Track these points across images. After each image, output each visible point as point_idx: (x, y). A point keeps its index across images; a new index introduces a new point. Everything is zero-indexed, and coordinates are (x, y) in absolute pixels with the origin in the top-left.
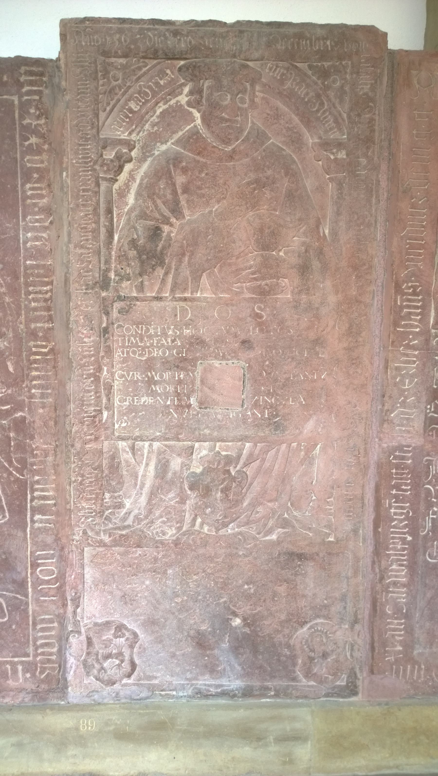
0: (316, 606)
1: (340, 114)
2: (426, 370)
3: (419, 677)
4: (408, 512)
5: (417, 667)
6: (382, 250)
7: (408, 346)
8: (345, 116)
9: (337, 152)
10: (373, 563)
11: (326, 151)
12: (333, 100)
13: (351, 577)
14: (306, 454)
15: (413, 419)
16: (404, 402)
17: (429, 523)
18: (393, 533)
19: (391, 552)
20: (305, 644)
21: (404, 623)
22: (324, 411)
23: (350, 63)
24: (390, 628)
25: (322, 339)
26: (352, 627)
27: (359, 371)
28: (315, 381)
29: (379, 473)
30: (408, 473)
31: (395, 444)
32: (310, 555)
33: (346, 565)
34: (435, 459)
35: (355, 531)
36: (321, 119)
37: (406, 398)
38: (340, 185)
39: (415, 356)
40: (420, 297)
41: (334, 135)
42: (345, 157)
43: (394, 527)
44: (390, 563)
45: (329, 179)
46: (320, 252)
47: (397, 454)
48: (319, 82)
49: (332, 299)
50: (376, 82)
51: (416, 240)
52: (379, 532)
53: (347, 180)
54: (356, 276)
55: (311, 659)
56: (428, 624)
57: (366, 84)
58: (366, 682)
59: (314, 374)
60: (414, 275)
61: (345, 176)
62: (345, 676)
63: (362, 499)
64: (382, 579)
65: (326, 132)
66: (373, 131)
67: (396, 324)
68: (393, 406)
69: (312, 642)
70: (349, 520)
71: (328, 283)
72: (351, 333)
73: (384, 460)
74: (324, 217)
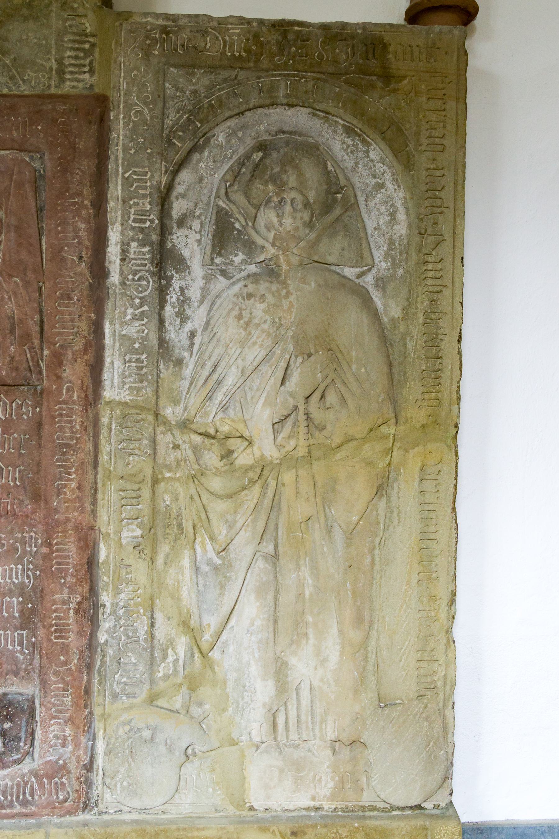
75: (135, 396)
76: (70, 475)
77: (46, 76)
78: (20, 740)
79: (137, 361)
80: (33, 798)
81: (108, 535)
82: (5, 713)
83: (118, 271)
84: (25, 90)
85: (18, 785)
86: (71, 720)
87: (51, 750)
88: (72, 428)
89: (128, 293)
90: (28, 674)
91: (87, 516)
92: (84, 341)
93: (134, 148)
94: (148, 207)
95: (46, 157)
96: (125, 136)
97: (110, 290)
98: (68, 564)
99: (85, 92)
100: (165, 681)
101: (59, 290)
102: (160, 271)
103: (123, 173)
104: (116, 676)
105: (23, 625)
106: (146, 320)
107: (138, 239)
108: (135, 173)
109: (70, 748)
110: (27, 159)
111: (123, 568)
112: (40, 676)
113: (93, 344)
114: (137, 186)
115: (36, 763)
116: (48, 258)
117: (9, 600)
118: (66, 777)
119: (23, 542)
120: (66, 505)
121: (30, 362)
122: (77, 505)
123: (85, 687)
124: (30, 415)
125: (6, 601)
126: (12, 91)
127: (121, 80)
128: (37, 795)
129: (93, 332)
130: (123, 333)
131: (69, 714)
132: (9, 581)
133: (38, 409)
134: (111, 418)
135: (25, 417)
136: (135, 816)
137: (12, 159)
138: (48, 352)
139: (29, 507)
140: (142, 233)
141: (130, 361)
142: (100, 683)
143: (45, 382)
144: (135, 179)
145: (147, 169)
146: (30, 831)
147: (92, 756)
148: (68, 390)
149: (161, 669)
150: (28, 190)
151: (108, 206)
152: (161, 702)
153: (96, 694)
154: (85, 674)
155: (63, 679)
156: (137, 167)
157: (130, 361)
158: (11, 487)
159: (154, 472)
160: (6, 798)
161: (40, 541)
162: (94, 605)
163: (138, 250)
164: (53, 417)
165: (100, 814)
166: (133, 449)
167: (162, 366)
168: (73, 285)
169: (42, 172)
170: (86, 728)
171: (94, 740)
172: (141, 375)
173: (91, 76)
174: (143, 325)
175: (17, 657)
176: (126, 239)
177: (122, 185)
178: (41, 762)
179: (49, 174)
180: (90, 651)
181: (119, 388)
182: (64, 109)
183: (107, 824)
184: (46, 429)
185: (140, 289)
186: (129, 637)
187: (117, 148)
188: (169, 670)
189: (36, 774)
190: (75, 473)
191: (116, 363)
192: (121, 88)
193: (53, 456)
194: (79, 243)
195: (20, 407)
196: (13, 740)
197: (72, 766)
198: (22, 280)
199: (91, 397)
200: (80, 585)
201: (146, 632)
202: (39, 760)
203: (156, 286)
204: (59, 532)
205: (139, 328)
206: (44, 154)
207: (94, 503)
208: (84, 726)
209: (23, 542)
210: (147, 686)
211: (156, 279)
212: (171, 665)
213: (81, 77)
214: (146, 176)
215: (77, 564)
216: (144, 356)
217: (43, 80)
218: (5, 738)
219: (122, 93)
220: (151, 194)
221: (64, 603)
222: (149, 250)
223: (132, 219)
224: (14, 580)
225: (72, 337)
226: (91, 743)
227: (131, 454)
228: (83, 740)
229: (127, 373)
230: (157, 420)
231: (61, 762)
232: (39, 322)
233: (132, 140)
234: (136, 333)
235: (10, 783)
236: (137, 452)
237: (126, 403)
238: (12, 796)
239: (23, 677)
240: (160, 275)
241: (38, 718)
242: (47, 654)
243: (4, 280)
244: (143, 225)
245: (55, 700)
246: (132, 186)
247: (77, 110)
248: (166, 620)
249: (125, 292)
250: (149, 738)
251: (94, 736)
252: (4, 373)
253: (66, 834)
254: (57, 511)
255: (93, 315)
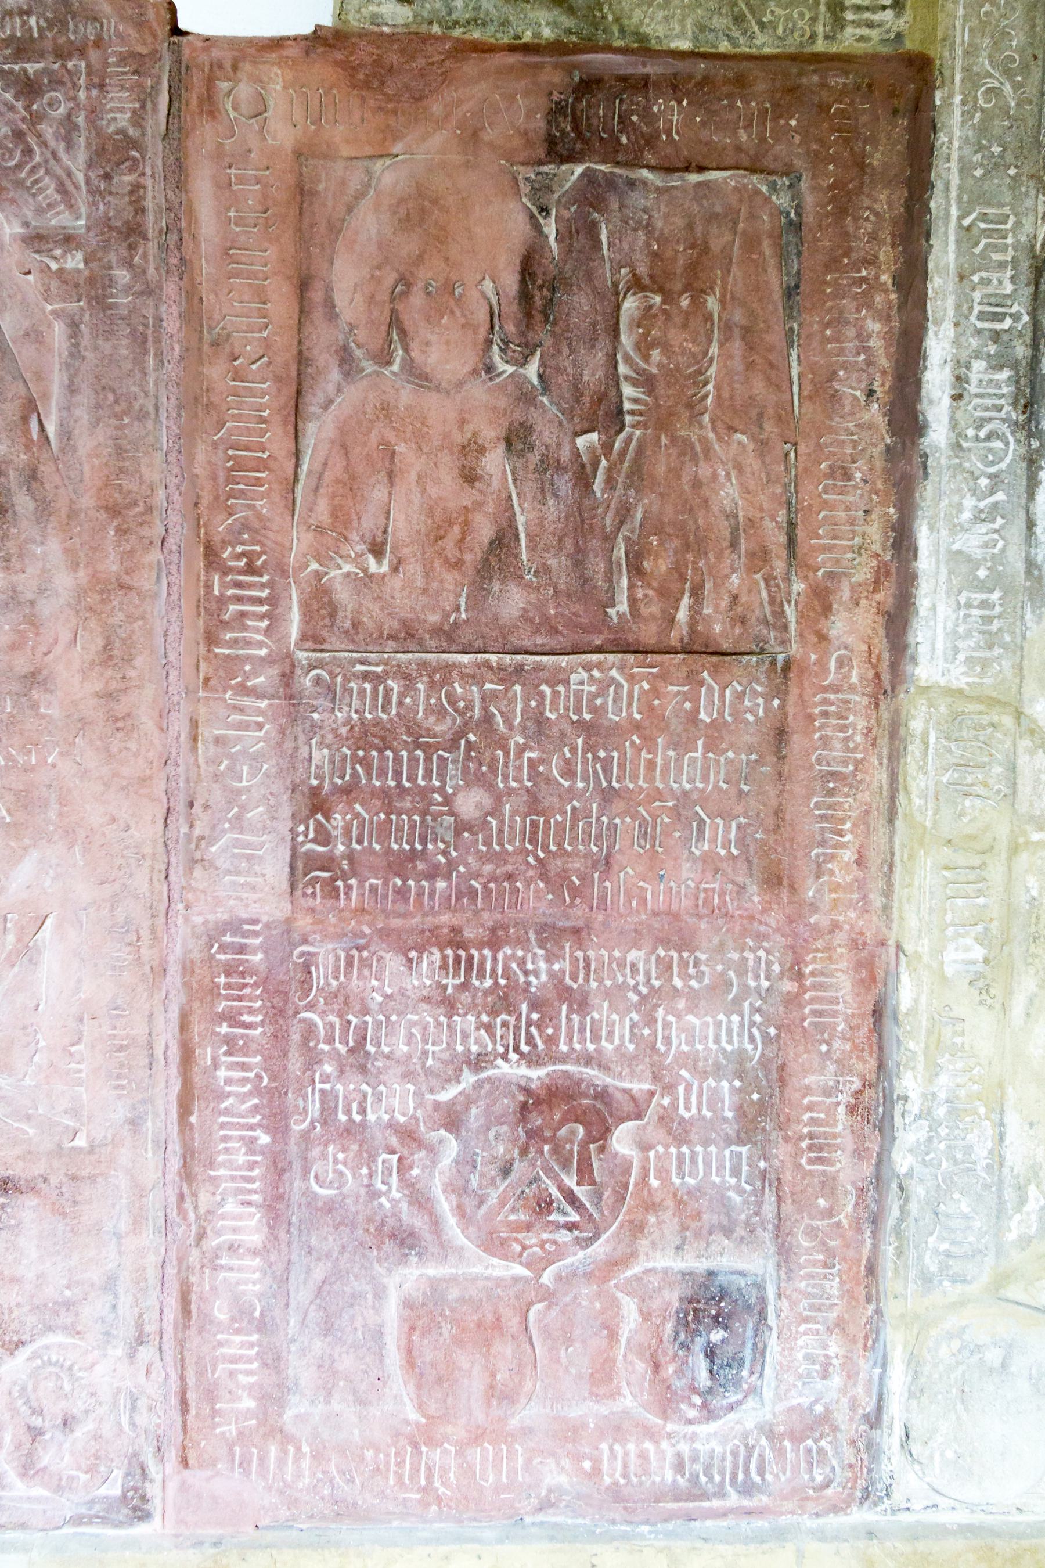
0: (45, 1305)
1: (69, 175)
2: (289, 745)
3: (298, 1475)
4: (259, 1077)
5: (291, 1449)
6: (176, 470)
7: (244, 690)
8: (80, 177)
9: (63, 256)
10: (181, 1197)
11: (37, 252)
12: (52, 143)
13: (127, 1234)
14: (19, 940)
15: (261, 857)
16: (238, 817)
17: (313, 1101)
18: (222, 1126)
19: (221, 1172)
20: (20, 1396)
21: (259, 1344)
22: (56, 838)
23: (83, 64)
24: (223, 1356)
25: (45, 672)
26: (132, 1355)
27: (133, 746)
28: (33, 769)
29: (187, 985)
30: (256, 985)
31: (222, 915)
32: (27, 1181)
33: (113, 1205)
34: (322, 951)
35: (135, 1123)
36: (28, 184)
37: (243, 808)
38: (74, 326)
39: (260, 712)
40: (265, 579)
41: (60, 219)
42: (81, 266)
43: (227, 1112)
44: (218, 1198)
45: (53, 312)
46: (32, 476)
47: (228, 939)
48: (19, 105)
49: (64, 581)
50: (143, 107)
51: (247, 449)
52: (191, 1125)
53: (87, 317)
54: (118, 530)
55: (35, 1433)
56: (318, 1345)
57: (122, 110)
58: (172, 1487)
59: (30, 751)
60: (246, 527)
61: (82, 308)
62: (118, 1474)
63: (150, 1046)
64: (201, 1236)
65: (40, 211)
66: (141, 211)
67: (211, 639)
68: (213, 828)
69: (35, 1390)
70: (119, 1097)
71: (54, 547)
72: (111, 658)
73: (196, 955)
74: (46, 396)
75: (978, 676)
76: (842, 836)
77: (807, 17)
78: (741, 1364)
79: (984, 604)
80: (763, 1480)
81: (918, 956)
82: (713, 1312)
83: (945, 420)
84: (764, 44)
85: (735, 1454)
86: (840, 1324)
87: (799, 1384)
88: (847, 739)
89: (967, 465)
90: (751, 1232)
91: (875, 918)
92: (874, 563)
93: (982, 165)
94: (1008, 288)
95: (804, 185)
96: (966, 141)
97: (930, 459)
98: (834, 1014)
99: (885, 50)
100: (1023, 1249)
101: (827, 459)
102: (1029, 420)
103: (961, 218)
104: (931, 1240)
105: (743, 1135)
106: (1000, 521)
107: (989, 356)
108: (984, 217)
109: (836, 1380)
110: (764, 189)
111: (947, 1023)
112: (777, 1237)
113: (893, 570)
114: (987, 246)
115: (768, 1408)
116: (805, 393)
117: (713, 1084)
118: (829, 1439)
119: (742, 970)
120: (834, 895)
121: (766, 605)
122: (855, 896)
123: (868, 1260)
124: (761, 714)
125: (708, 1085)
126: (739, 46)
127: (958, 24)
128: (772, 1473)
129: (893, 546)
130: (956, 547)
131: (835, 1315)
132: (714, 1047)
133: (776, 702)
134: (927, 721)
135: (750, 718)
136: (962, 1517)
137: (735, 188)
138: (802, 586)
139: (756, 899)
140: (995, 342)
141: (969, 605)
142: (899, 1253)
143: (794, 646)
144: (985, 230)
145: (1007, 210)
146: (765, 1546)
147: (880, 1398)
148: (840, 663)
149: (1013, 1224)
150: (767, 253)
151: (929, 286)
152: (1014, 1292)
153: (890, 1274)
154: (868, 1234)
155: (824, 1243)
156: (989, 204)
157: (969, 605)
158: (721, 859)
159: (1012, 831)
160: (711, 1478)
161: (776, 968)
162: (884, 1097)
163: (986, 377)
164: (811, 718)
165: (894, 1512)
166: (972, 785)
167: (1028, 616)
168: (854, 448)
169: (792, 215)
170: (870, 1342)
171: (884, 1365)
172: (989, 633)
173: (898, 15)
174: (997, 531)
175: (729, 1198)
176: (964, 355)
177: (958, 242)
178: (780, 1407)
179: (809, 219)
180: (877, 1188)
181: (946, 660)
182: (845, 84)
183: (915, 1534)
184: (796, 742)
185: (991, 458)
186: (956, 1162)
187: (947, 165)
188: (1029, 1227)
189: (771, 1431)
190: (852, 832)
191: (941, 609)
192: (958, 40)
193: (809, 798)
194: (869, 363)
195: (740, 696)
196: (729, 1365)
197: (841, 1417)
198: (753, 438)
199: (886, 677)
200: (858, 1058)
201: (991, 1152)
202: (774, 1404)
203: (1023, 450)
204: (817, 950)
205: (986, 538)
206: (799, 179)
207: (888, 893)
208: (866, 1337)
209: (742, 970)
210: (990, 1260)
211: (1021, 435)
212: (1034, 1217)
213: (876, 17)
214: (1005, 223)
215: (853, 1015)
216: (996, 596)
217: (800, 24)
218: (712, 1362)
219: (959, 51)
220: (1015, 261)
221: (827, 1092)
222: (1009, 378)
223: (976, 312)
224: (724, 1044)
225: (849, 556)
226: (878, 1371)
227: (967, 795)
228: (864, 1365)
229: (961, 630)
230: (1019, 724)
231: (819, 1409)
232: (785, 525)
233: (980, 148)
234: (982, 547)
235: (718, 1450)
236: (980, 790)
237: (960, 691)
238: (722, 1473)
239: (742, 1239)
240: (1030, 429)
241: (772, 1320)
242: (792, 1194)
243: (720, 439)
244: (998, 326)
245: (808, 1285)
246: (977, 244)
247: (869, 86)
248: (1026, 1127)
249: (960, 465)
250: (997, 1363)
251: (885, 1356)
252: (717, 628)
253: (837, 1553)
254: (814, 908)
255: (892, 510)
